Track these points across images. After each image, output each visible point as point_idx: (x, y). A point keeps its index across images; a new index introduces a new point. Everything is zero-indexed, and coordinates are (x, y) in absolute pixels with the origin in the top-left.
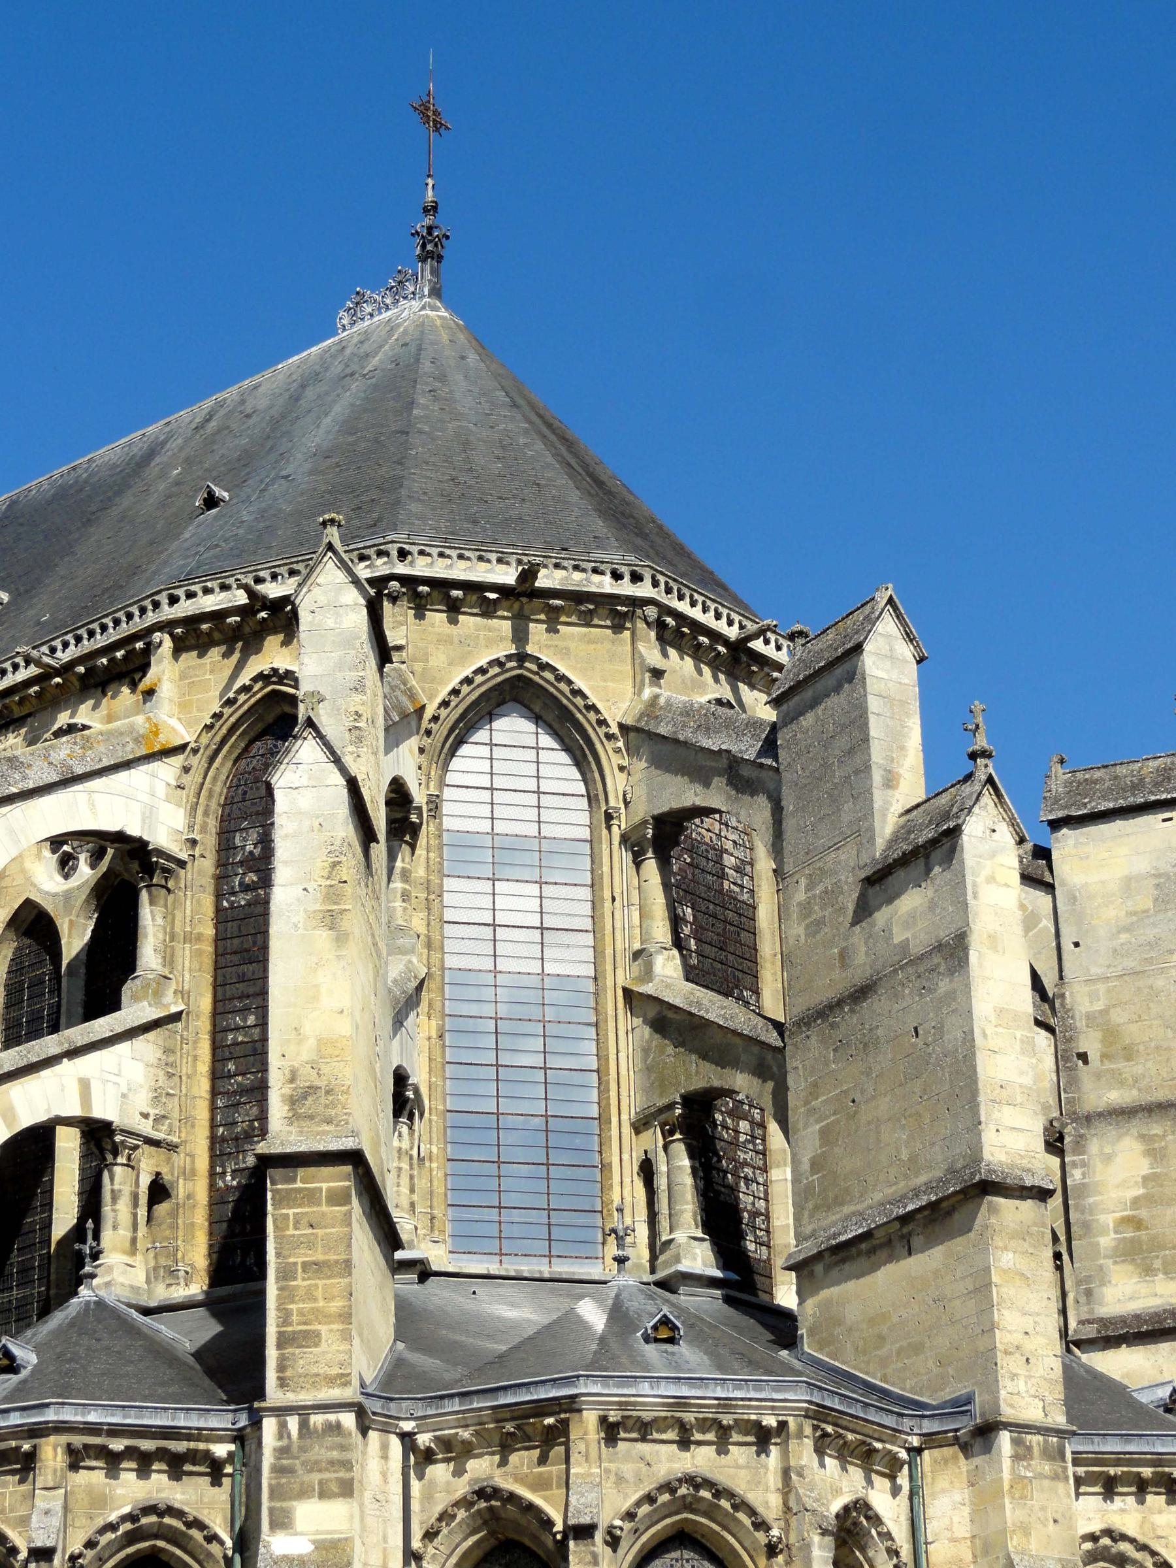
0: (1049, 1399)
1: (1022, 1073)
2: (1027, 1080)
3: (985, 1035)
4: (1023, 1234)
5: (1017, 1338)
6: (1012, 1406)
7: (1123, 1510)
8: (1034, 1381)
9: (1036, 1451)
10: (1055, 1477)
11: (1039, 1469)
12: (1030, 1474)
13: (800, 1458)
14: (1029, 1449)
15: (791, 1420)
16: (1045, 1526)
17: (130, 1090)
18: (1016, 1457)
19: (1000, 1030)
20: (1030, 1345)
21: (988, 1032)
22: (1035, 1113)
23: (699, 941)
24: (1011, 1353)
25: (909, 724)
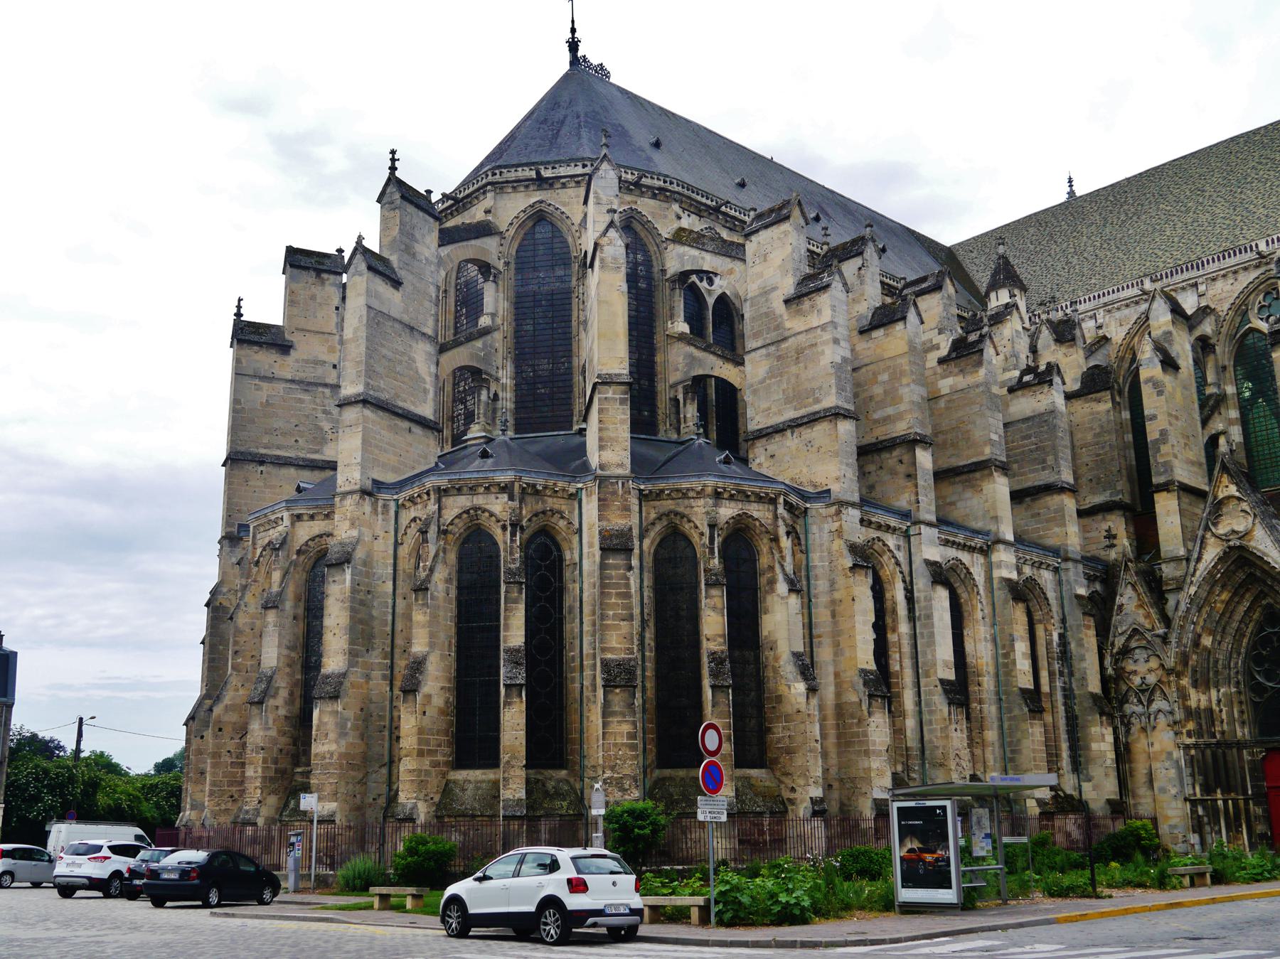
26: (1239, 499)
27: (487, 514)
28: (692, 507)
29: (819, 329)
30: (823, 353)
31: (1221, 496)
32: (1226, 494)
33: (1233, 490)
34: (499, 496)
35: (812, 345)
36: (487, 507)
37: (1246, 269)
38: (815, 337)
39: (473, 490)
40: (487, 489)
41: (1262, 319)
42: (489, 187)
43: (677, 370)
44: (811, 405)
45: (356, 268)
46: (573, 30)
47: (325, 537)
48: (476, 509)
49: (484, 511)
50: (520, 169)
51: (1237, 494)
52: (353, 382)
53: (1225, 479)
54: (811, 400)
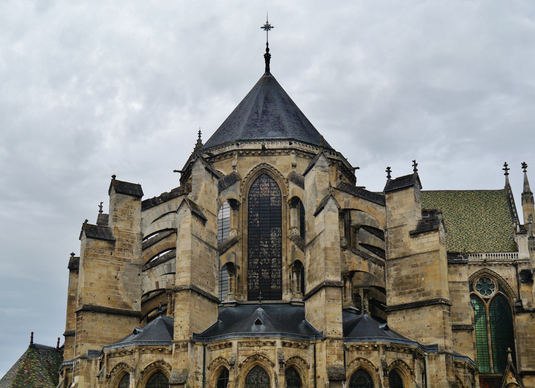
0: (185, 334)
1: (187, 264)
2: (188, 265)
3: (178, 258)
4: (183, 300)
5: (179, 323)
6: (176, 338)
7: (223, 352)
8: (182, 331)
9: (181, 346)
10: (185, 351)
11: (181, 350)
12: (179, 352)
13: (134, 357)
14: (179, 346)
15: (134, 349)
16: (181, 362)
17: (169, 281)
18: (176, 349)
19: (183, 256)
20: (182, 324)
21: (179, 257)
22: (189, 272)
23: (259, 220)
24: (177, 327)
25: (202, 183)
26: (517, 385)
27: (403, 364)
28: (458, 372)
29: (461, 284)
30: (463, 296)
31: (508, 382)
32: (511, 382)
33: (514, 380)
34: (409, 355)
35: (456, 291)
36: (404, 360)
37: (475, 265)
38: (458, 287)
39: (398, 350)
40: (405, 350)
41: (478, 291)
42: (293, 151)
43: (359, 279)
44: (455, 321)
45: (330, 207)
46: (268, 50)
47: (296, 359)
48: (400, 360)
49: (403, 362)
50: (308, 146)
51: (516, 382)
52: (333, 274)
53: (511, 374)
54: (456, 318)
